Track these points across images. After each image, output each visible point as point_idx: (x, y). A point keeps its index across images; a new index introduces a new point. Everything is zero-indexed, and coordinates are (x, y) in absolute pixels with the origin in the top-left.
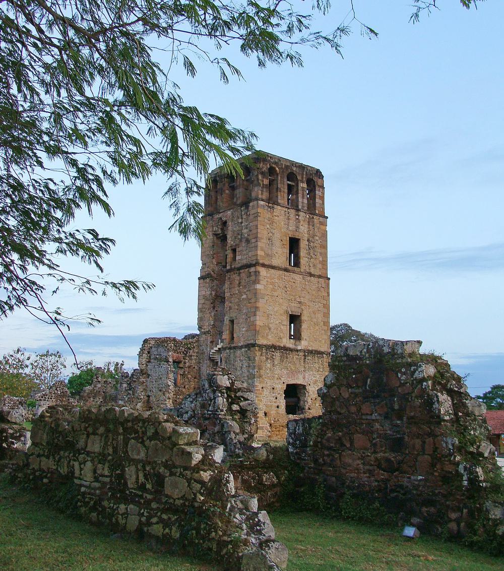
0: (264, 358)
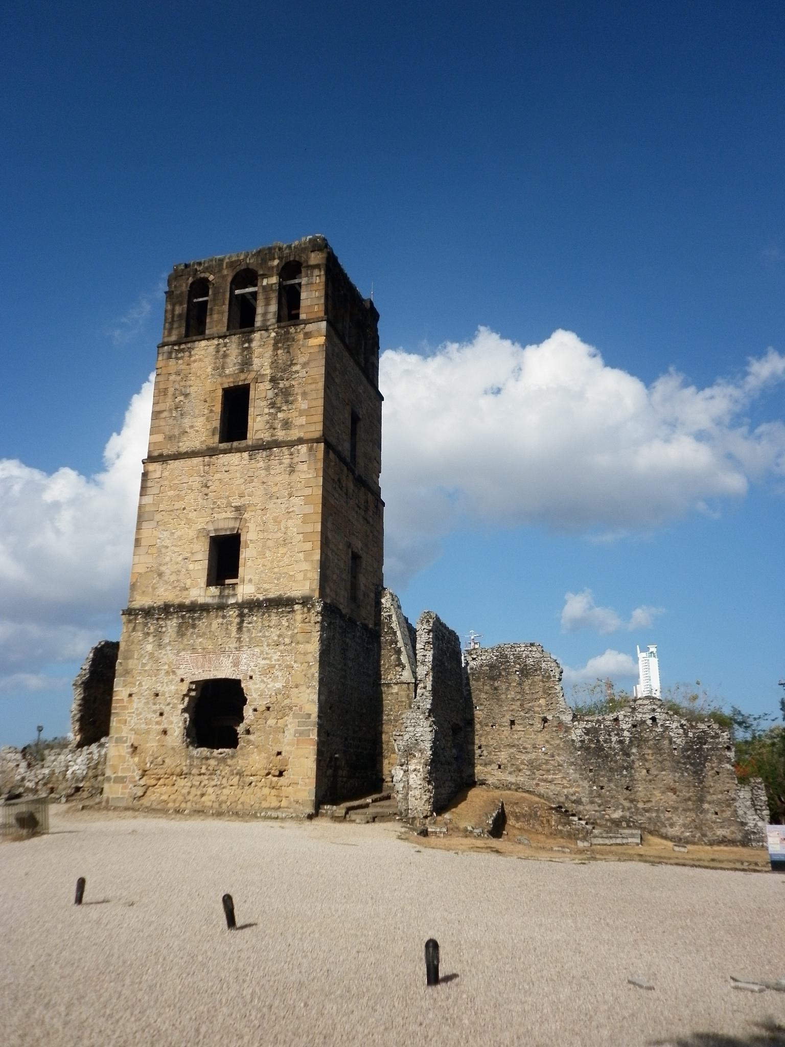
0: (140, 634)
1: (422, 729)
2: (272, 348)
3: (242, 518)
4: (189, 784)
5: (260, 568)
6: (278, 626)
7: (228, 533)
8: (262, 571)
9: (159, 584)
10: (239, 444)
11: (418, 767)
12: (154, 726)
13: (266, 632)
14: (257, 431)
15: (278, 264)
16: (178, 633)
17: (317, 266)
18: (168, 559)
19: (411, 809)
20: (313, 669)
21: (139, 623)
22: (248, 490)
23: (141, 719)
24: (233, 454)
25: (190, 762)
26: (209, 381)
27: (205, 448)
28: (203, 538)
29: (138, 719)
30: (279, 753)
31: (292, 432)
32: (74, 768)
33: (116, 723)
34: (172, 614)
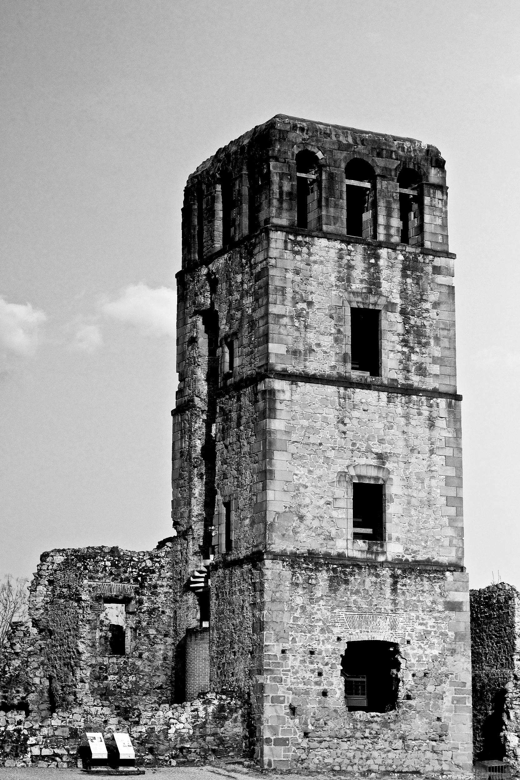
3: (384, 468)
4: (354, 748)
7: (372, 482)
8: (408, 531)
12: (313, 687)
13: (421, 597)
14: (391, 369)
16: (330, 586)
23: (298, 678)
24: (371, 392)
25: (354, 726)
26: (334, 293)
27: (337, 376)
28: (345, 484)
29: (295, 678)
30: (439, 719)
31: (427, 379)
32: (177, 727)
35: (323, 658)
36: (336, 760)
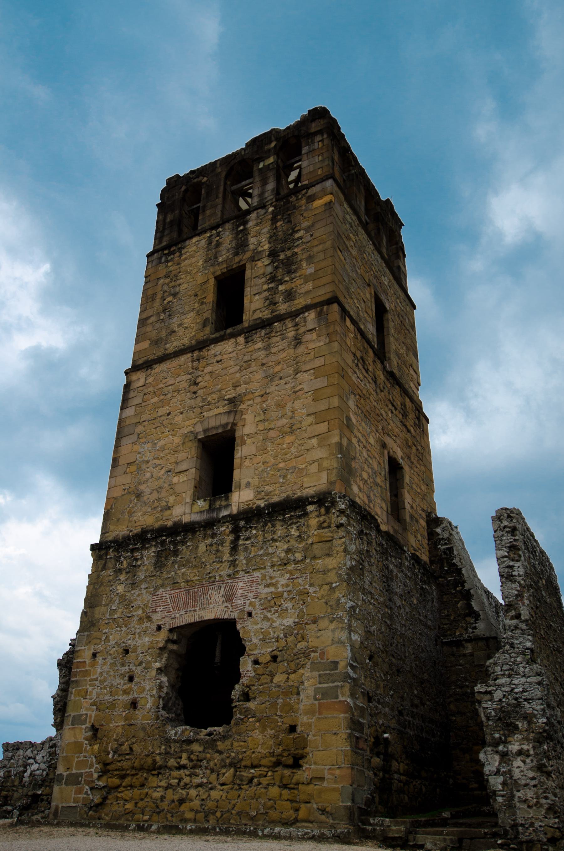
0: (110, 572)
1: (523, 680)
2: (270, 223)
3: (236, 411)
4: (163, 783)
5: (261, 467)
6: (286, 538)
7: (220, 431)
9: (136, 508)
10: (234, 329)
11: (525, 747)
12: (120, 698)
14: (254, 311)
15: (275, 146)
16: (155, 564)
17: (320, 132)
18: (148, 475)
19: (522, 825)
20: (337, 592)
21: (111, 558)
22: (243, 377)
24: (227, 341)
25: (165, 749)
26: (200, 274)
28: (190, 444)
31: (296, 302)
33: (75, 695)
34: (149, 541)
35: (137, 656)
36: (139, 805)
